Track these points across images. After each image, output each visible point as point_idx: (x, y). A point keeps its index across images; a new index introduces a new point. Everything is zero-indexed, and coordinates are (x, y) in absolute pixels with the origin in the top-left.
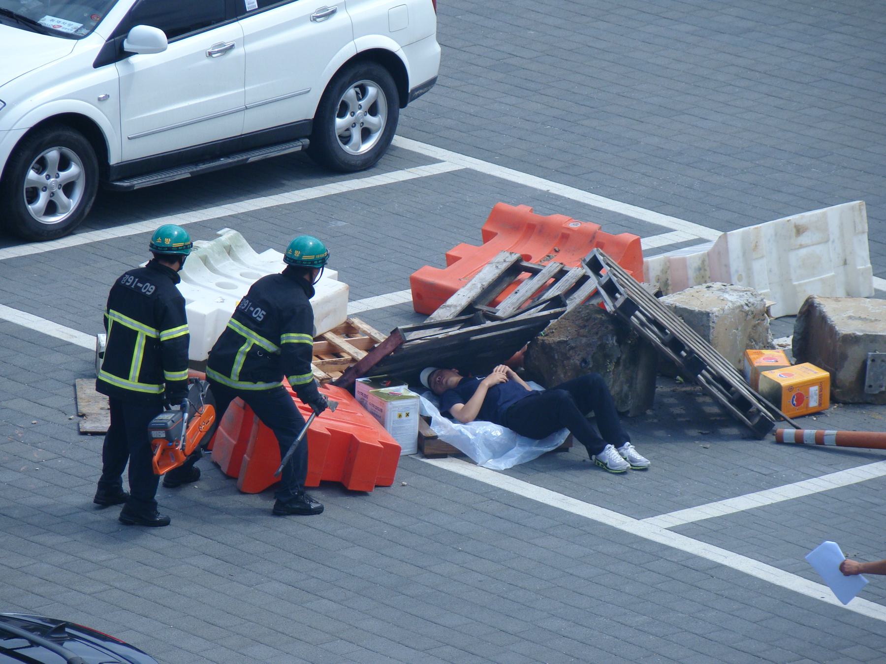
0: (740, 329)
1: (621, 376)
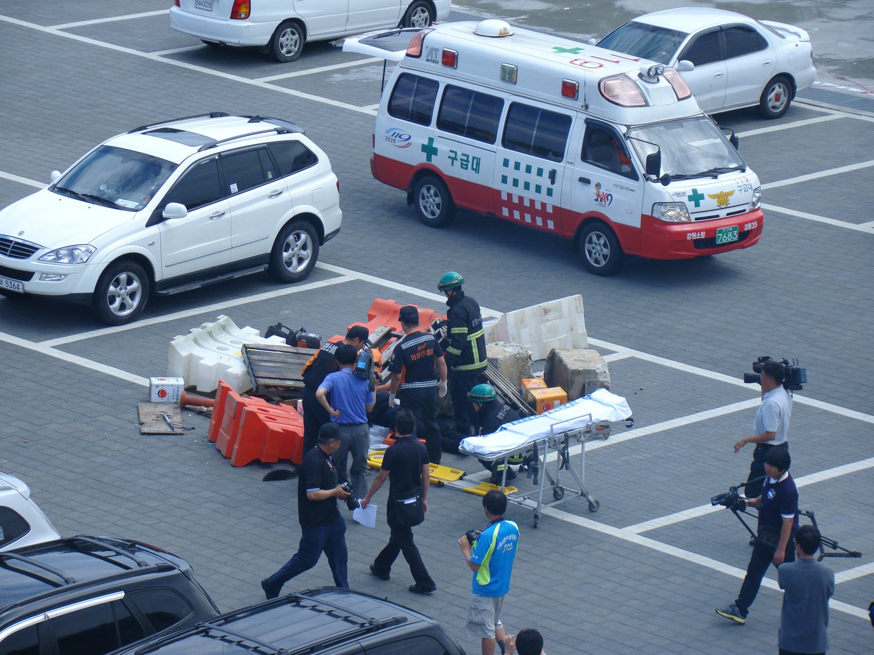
0: (514, 368)
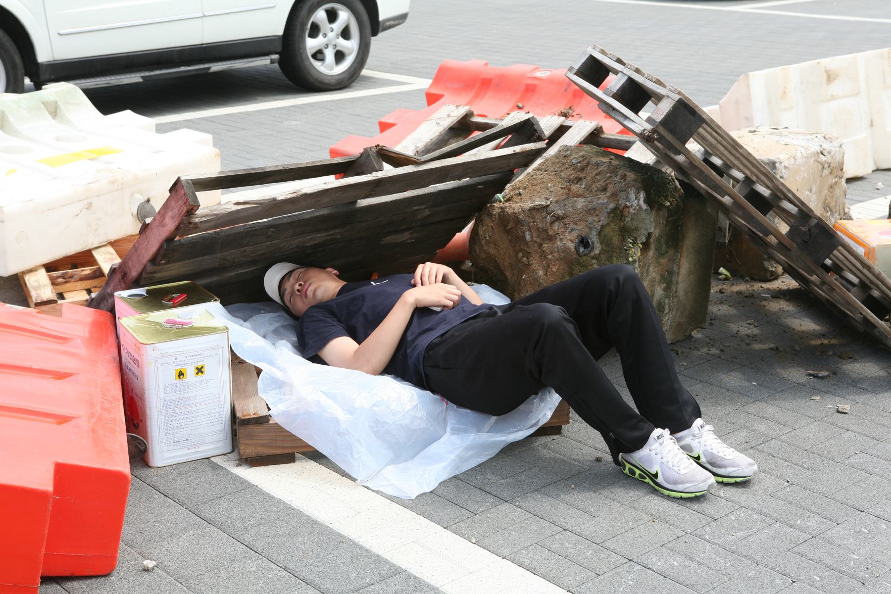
0: (814, 189)
1: (651, 269)
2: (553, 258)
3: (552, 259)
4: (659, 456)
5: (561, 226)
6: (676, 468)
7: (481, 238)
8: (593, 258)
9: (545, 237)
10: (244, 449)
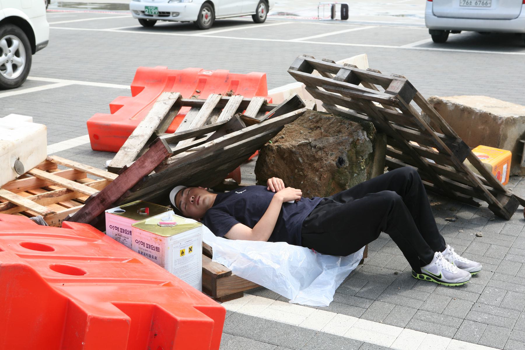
2: (323, 170)
3: (323, 171)
4: (441, 266)
5: (322, 153)
6: (451, 271)
7: (268, 163)
8: (345, 169)
9: (313, 159)
10: (219, 292)
